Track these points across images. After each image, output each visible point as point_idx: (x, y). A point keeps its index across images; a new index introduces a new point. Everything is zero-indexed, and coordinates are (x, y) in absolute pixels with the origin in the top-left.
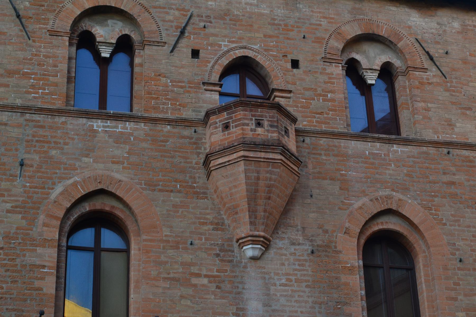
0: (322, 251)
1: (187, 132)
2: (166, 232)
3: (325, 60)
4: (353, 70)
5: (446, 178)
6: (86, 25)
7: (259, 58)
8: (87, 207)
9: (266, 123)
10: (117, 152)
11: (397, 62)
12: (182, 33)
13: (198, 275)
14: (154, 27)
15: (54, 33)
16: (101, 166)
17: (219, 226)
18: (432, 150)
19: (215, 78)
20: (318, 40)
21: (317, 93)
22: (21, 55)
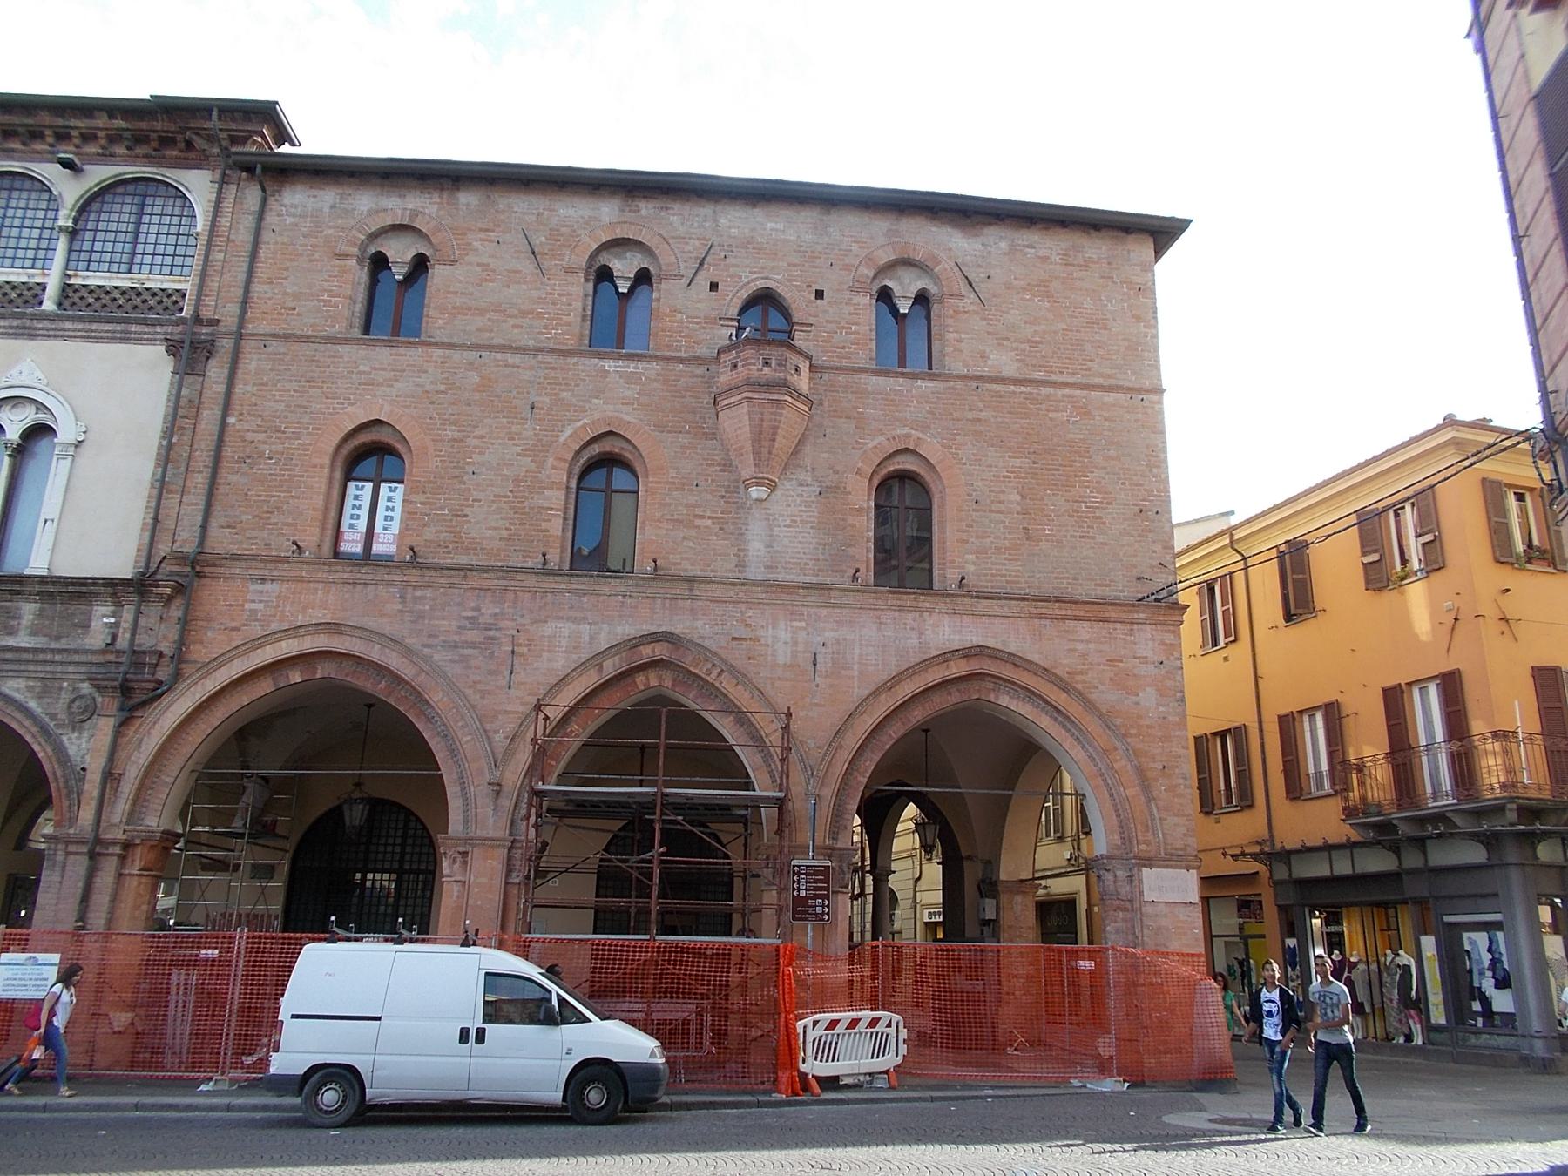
0: (830, 492)
1: (700, 371)
2: (673, 473)
3: (851, 289)
4: (885, 296)
5: (970, 415)
6: (604, 259)
7: (781, 290)
8: (596, 449)
9: (773, 363)
10: (628, 393)
11: (933, 289)
12: (701, 264)
13: (702, 517)
14: (673, 259)
15: (569, 270)
16: (611, 407)
17: (727, 466)
18: (959, 385)
19: (734, 312)
20: (847, 268)
21: (840, 324)
22: (535, 294)
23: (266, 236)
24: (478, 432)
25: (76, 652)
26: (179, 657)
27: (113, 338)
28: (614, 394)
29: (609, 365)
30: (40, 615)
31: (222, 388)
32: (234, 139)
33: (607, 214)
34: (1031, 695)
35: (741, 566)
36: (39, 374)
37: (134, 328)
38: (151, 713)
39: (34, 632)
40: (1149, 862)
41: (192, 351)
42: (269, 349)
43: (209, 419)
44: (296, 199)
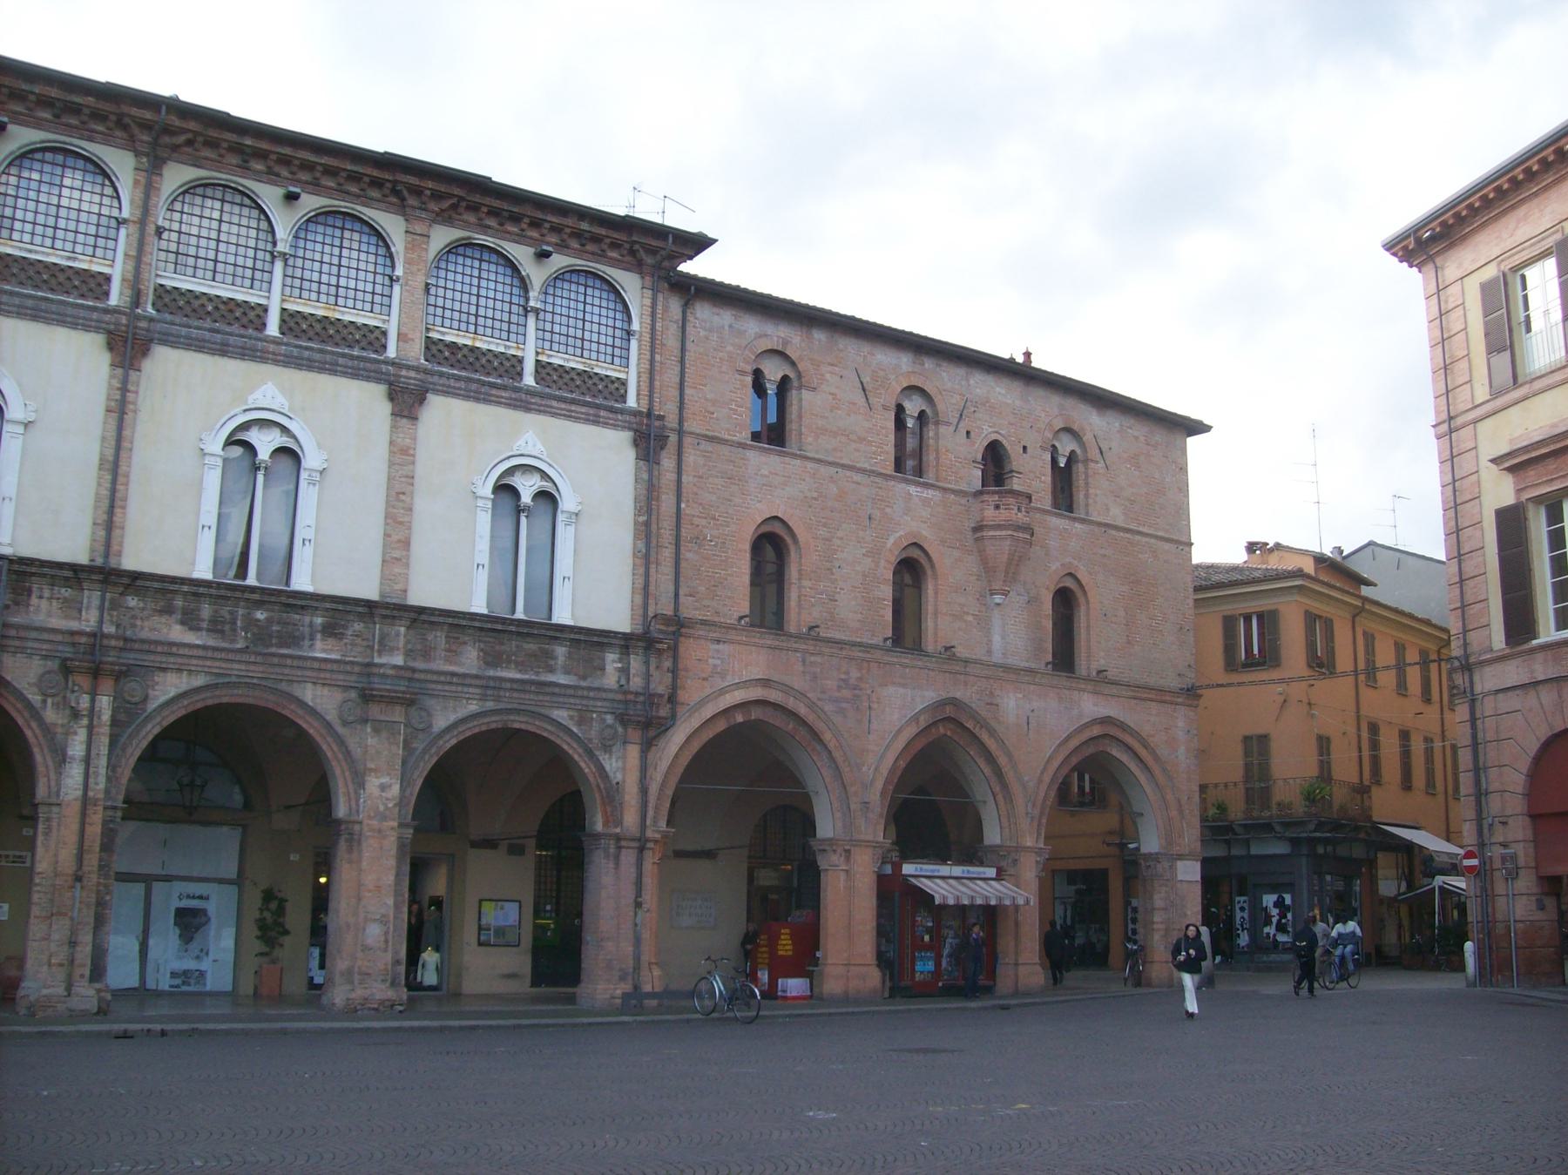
0: (1032, 601)
1: (963, 501)
5: (1102, 551)
18: (1096, 529)
21: (1033, 474)
23: (689, 345)
24: (840, 534)
25: (599, 689)
26: (672, 699)
27: (587, 421)
28: (915, 513)
29: (912, 489)
30: (570, 656)
31: (673, 476)
32: (657, 250)
33: (902, 364)
35: (989, 652)
36: (540, 446)
37: (602, 413)
38: (662, 743)
39: (567, 672)
41: (650, 439)
42: (702, 447)
43: (667, 502)
44: (704, 313)
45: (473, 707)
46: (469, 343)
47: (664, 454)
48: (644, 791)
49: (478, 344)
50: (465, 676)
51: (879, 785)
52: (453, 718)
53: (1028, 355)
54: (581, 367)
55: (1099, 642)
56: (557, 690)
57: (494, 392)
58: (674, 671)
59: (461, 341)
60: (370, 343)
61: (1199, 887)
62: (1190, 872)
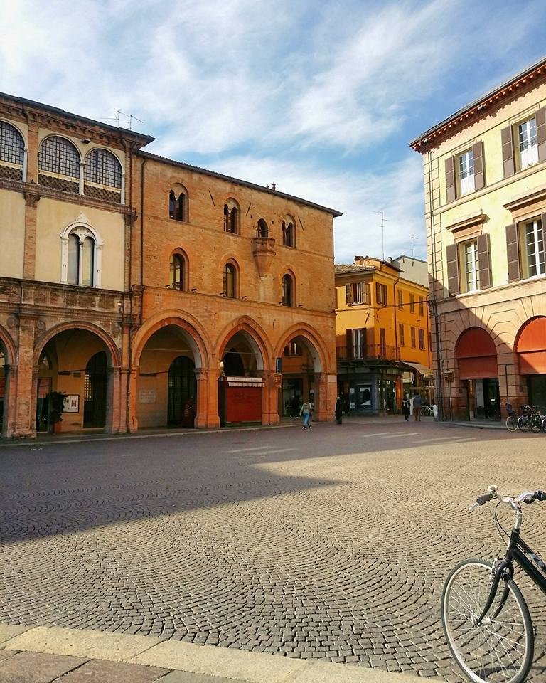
21: (276, 232)
23: (145, 180)
25: (112, 313)
26: (140, 317)
29: (230, 237)
30: (101, 301)
31: (140, 232)
32: (131, 142)
34: (310, 334)
35: (259, 299)
36: (87, 219)
37: (111, 207)
39: (100, 306)
40: (329, 374)
41: (130, 218)
44: (150, 167)
45: (62, 321)
46: (57, 177)
47: (136, 222)
48: (130, 351)
49: (60, 178)
50: (59, 308)
51: (218, 348)
52: (54, 325)
53: (274, 185)
54: (102, 188)
55: (300, 297)
56: (96, 314)
57: (68, 197)
58: (141, 306)
59: (53, 176)
60: (16, 176)
61: (336, 385)
62: (333, 379)
